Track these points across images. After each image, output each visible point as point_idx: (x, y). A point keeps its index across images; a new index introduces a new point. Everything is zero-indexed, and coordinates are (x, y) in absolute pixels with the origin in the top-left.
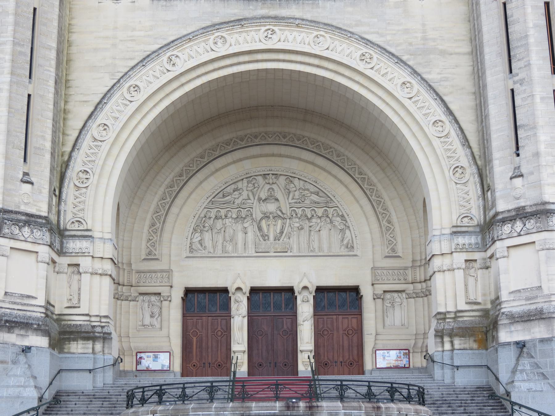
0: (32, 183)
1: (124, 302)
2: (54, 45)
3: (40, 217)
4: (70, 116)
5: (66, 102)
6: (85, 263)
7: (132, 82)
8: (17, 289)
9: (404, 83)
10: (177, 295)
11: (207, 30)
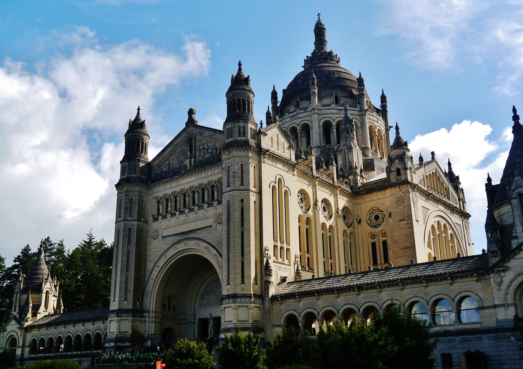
0: (127, 301)
1: (183, 325)
2: (134, 259)
3: (130, 309)
5: (145, 272)
6: (147, 319)
7: (158, 264)
8: (122, 330)
9: (215, 255)
10: (197, 321)
11: (172, 246)
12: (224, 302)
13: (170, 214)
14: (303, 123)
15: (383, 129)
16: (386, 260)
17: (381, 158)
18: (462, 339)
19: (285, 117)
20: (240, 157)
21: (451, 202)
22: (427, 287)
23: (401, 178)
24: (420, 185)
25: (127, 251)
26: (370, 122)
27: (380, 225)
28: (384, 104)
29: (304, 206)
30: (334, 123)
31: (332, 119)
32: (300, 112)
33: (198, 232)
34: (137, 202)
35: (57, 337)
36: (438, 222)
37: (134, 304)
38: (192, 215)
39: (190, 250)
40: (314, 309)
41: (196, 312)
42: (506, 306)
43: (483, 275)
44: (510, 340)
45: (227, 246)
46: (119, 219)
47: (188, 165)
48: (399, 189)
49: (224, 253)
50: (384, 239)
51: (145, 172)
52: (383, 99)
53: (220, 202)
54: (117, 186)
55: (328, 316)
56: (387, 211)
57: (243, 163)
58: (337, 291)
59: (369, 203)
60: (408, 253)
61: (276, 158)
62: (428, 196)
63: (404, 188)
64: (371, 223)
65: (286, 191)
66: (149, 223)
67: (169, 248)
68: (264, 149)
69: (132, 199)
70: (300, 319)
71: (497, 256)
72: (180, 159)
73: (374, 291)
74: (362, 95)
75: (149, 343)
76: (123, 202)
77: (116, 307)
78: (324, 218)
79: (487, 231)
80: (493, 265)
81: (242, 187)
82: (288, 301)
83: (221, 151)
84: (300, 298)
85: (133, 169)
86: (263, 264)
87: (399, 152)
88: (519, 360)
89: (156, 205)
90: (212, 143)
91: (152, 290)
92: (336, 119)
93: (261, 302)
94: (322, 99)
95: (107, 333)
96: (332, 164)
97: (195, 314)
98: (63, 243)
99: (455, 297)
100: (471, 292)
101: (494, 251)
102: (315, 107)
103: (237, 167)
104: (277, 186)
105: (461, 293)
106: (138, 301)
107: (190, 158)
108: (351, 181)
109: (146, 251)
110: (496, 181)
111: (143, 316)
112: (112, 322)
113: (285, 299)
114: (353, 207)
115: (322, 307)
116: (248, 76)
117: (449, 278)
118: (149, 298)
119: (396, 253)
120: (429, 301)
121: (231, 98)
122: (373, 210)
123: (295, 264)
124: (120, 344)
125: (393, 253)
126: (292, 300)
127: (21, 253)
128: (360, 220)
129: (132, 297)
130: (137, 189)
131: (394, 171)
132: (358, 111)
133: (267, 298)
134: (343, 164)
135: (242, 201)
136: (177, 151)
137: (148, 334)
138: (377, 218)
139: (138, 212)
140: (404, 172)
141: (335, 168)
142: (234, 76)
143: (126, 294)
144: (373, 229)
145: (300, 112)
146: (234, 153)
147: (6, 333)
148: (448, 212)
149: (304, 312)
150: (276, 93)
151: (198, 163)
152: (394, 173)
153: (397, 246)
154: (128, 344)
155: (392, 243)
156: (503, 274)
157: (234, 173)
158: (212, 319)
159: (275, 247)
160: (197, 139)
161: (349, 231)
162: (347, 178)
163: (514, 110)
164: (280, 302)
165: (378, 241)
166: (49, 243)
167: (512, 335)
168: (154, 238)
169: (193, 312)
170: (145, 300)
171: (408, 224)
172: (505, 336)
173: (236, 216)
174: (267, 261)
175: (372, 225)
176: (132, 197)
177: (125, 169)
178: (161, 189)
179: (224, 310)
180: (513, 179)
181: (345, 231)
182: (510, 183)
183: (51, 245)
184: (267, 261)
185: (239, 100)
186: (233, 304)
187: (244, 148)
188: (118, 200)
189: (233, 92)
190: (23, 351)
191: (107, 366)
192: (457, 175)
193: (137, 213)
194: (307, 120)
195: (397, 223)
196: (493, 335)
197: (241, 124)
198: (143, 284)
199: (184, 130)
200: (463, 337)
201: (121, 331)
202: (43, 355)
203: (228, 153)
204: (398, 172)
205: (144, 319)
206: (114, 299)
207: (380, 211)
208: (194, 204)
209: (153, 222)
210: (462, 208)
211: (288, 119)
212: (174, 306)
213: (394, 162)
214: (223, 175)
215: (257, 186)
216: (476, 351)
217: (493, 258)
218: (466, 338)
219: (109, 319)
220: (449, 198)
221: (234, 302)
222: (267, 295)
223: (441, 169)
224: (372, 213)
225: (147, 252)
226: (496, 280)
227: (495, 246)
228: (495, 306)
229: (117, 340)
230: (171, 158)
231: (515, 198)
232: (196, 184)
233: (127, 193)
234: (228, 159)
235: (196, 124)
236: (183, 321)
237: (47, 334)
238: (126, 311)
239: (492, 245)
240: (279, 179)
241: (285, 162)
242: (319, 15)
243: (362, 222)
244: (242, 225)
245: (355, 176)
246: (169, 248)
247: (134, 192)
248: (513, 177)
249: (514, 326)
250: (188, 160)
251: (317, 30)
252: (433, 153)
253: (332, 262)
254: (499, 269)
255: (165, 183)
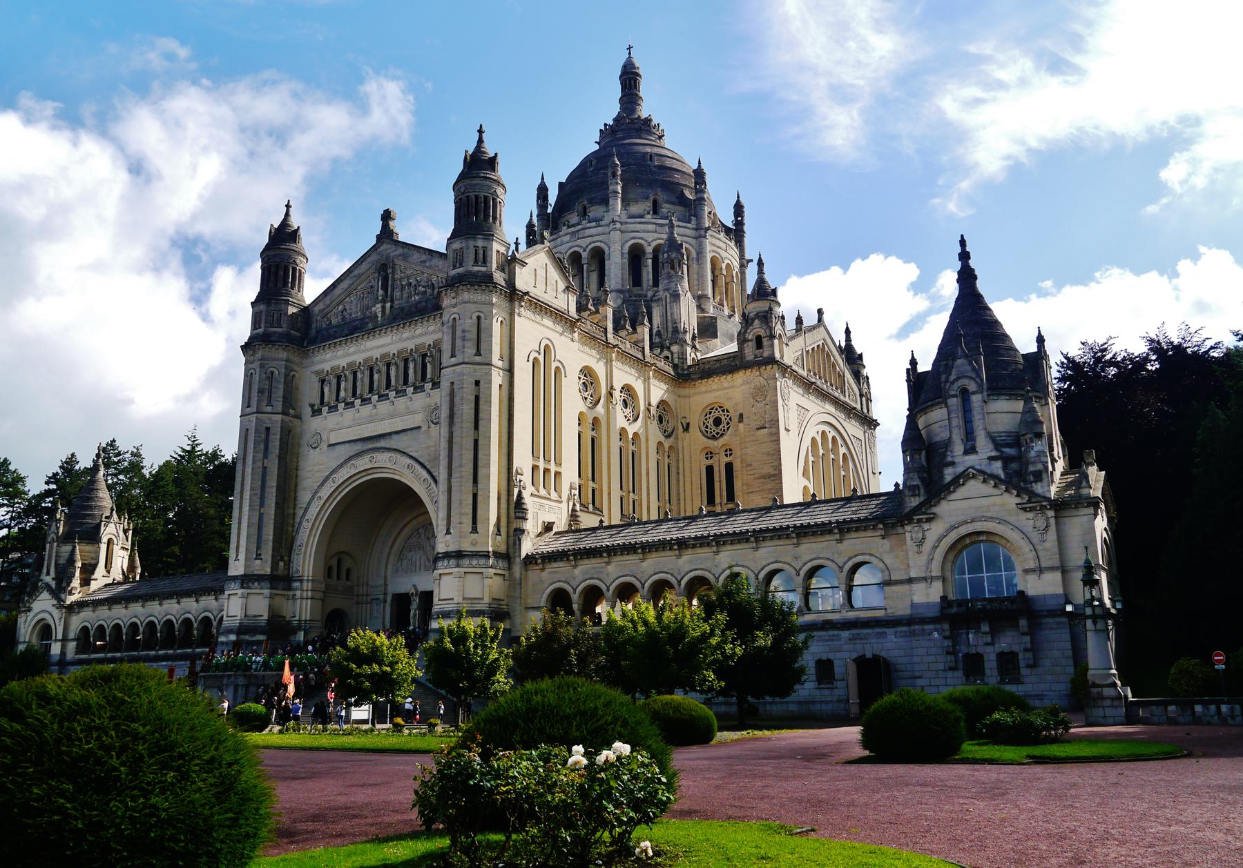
0: (261, 559)
2: (275, 484)
3: (266, 575)
4: (296, 516)
5: (295, 508)
6: (298, 593)
7: (319, 495)
8: (251, 612)
10: (389, 598)
12: (440, 564)
13: (343, 404)
14: (593, 245)
15: (736, 264)
16: (731, 497)
17: (730, 316)
18: (853, 635)
19: (561, 233)
20: (475, 303)
21: (847, 400)
22: (797, 545)
23: (763, 353)
24: (795, 368)
25: (261, 469)
26: (713, 251)
27: (722, 434)
28: (739, 219)
29: (589, 397)
30: (649, 250)
31: (646, 241)
32: (589, 225)
33: (394, 437)
34: (282, 380)
35: (128, 624)
36: (823, 432)
37: (274, 566)
38: (384, 407)
39: (378, 470)
40: (600, 580)
41: (388, 583)
42: (929, 580)
43: (894, 526)
44: (932, 637)
45: (446, 465)
46: (248, 410)
47: (380, 315)
48: (758, 373)
49: (442, 476)
50: (728, 459)
51: (299, 324)
52: (739, 209)
53: (436, 385)
54: (245, 348)
55: (626, 592)
56: (736, 411)
57: (482, 315)
58: (642, 550)
59: (705, 396)
60: (769, 486)
61: (541, 308)
62: (808, 386)
63: (768, 370)
64: (707, 432)
65: (557, 368)
66: (303, 418)
67: (341, 466)
68: (520, 291)
69: (272, 373)
70: (575, 597)
71: (919, 495)
72: (365, 302)
73: (706, 550)
74: (700, 201)
75: (301, 636)
76: (256, 378)
77: (241, 571)
78: (625, 420)
79: (904, 452)
80: (909, 512)
81: (478, 359)
82: (555, 565)
83: (441, 292)
84: (575, 559)
85: (275, 318)
86: (511, 498)
87: (761, 306)
88: (945, 670)
89: (317, 385)
90: (426, 275)
91: (307, 542)
92: (652, 241)
93: (506, 565)
94: (629, 204)
95: (222, 617)
96: (643, 324)
97: (386, 585)
98: (141, 451)
99: (845, 564)
100: (871, 555)
101: (914, 486)
102: (616, 218)
103: (470, 321)
104: (541, 358)
105: (855, 556)
106: (282, 559)
107: (384, 301)
108: (676, 355)
109: (297, 470)
110: (925, 366)
111: (290, 588)
112: (232, 597)
113: (550, 562)
114: (676, 400)
115: (615, 577)
116: (496, 154)
117: (836, 531)
118: (302, 556)
119: (747, 485)
120: (800, 569)
121: (463, 194)
122: (711, 408)
123: (569, 500)
124: (247, 637)
125: (743, 484)
126: (561, 564)
127: (61, 467)
128: (688, 424)
129: (270, 552)
130: (284, 355)
131: (751, 340)
132: (693, 229)
133: (517, 560)
134: (662, 323)
135: (477, 383)
136: (359, 287)
137: (299, 621)
138: (717, 422)
139: (284, 397)
140: (769, 343)
141: (647, 330)
142: (470, 152)
143: (258, 548)
144: (711, 442)
145: (589, 225)
146: (466, 295)
147: (31, 614)
148: (841, 416)
149: (583, 585)
150: (547, 190)
151: (399, 311)
152: (750, 343)
153: (751, 473)
154: (262, 637)
155: (742, 467)
156: (926, 526)
157: (463, 331)
158: (416, 594)
159: (535, 468)
160: (397, 267)
161: (667, 444)
162: (669, 348)
163: (963, 243)
164: (541, 566)
165: (717, 464)
166: (114, 450)
167: (936, 630)
168: (314, 446)
169: (381, 582)
170: (295, 558)
171: (771, 434)
172: (923, 630)
173: (465, 411)
174: (520, 493)
175: (709, 435)
176: (272, 369)
177: (260, 316)
178: (328, 356)
179: (440, 579)
180: (953, 363)
181: (660, 443)
182: (948, 369)
183: (119, 454)
184: (520, 493)
185: (477, 197)
186: (457, 569)
187: (484, 288)
188: (246, 375)
189: (467, 182)
190: (63, 648)
191: (222, 677)
192: (859, 352)
193: (281, 399)
194: (601, 242)
195: (752, 433)
196: (905, 629)
197: (480, 243)
198: (290, 529)
199: (374, 248)
200: (854, 631)
201: (248, 613)
202: (102, 655)
203: (453, 295)
204: (759, 340)
205: (291, 593)
206: (237, 557)
207: (723, 411)
208: (388, 386)
209: (312, 416)
210: (865, 411)
211: (567, 238)
212: (348, 571)
213: (752, 324)
214: (443, 333)
215: (506, 358)
216: (873, 655)
217: (912, 499)
218: (859, 634)
219: (227, 593)
220: (843, 392)
221: (458, 566)
222: (517, 554)
223: (832, 340)
224: (710, 413)
225: (299, 472)
226: (914, 535)
227: (916, 477)
228: (910, 581)
229: (242, 630)
230: (348, 299)
231: (955, 396)
232: (393, 350)
233: (263, 362)
234: (454, 306)
235: (395, 238)
236: (364, 598)
237: (109, 618)
238: (260, 578)
239: (911, 475)
240: (547, 346)
241: (558, 315)
242: (630, 48)
243: (691, 429)
244: (476, 427)
245: (682, 346)
246: (341, 466)
247: (277, 360)
248: (954, 360)
249: (938, 614)
250: (379, 306)
251: (625, 77)
252: (820, 312)
253: (636, 497)
254: (921, 517)
255: (335, 347)
